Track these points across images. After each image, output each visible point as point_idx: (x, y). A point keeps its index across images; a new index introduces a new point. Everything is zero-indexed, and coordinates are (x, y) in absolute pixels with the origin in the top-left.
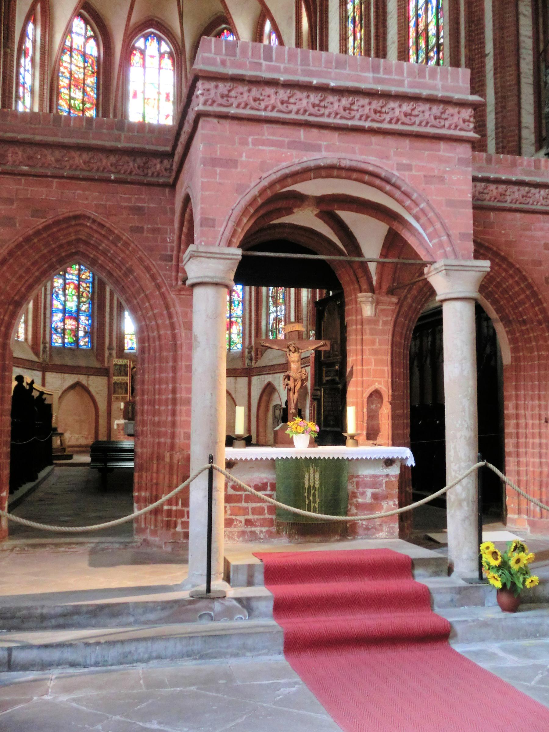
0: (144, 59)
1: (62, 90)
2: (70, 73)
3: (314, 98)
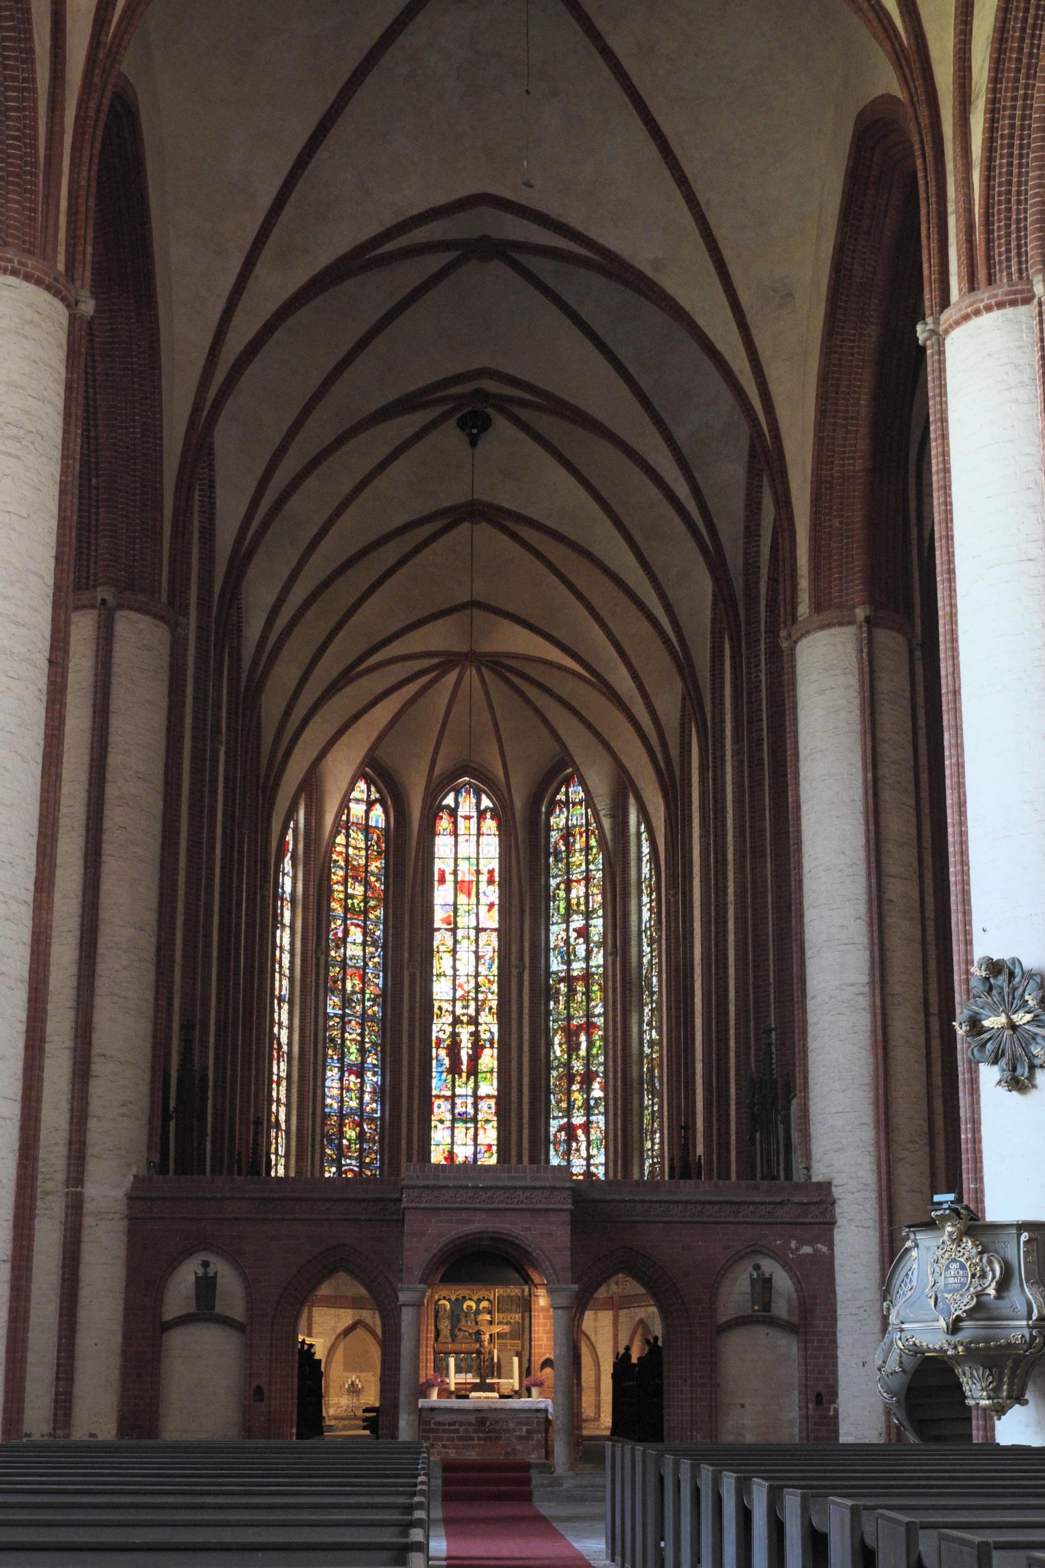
0: (455, 824)
1: (335, 887)
2: (347, 860)
3: (470, 1193)
